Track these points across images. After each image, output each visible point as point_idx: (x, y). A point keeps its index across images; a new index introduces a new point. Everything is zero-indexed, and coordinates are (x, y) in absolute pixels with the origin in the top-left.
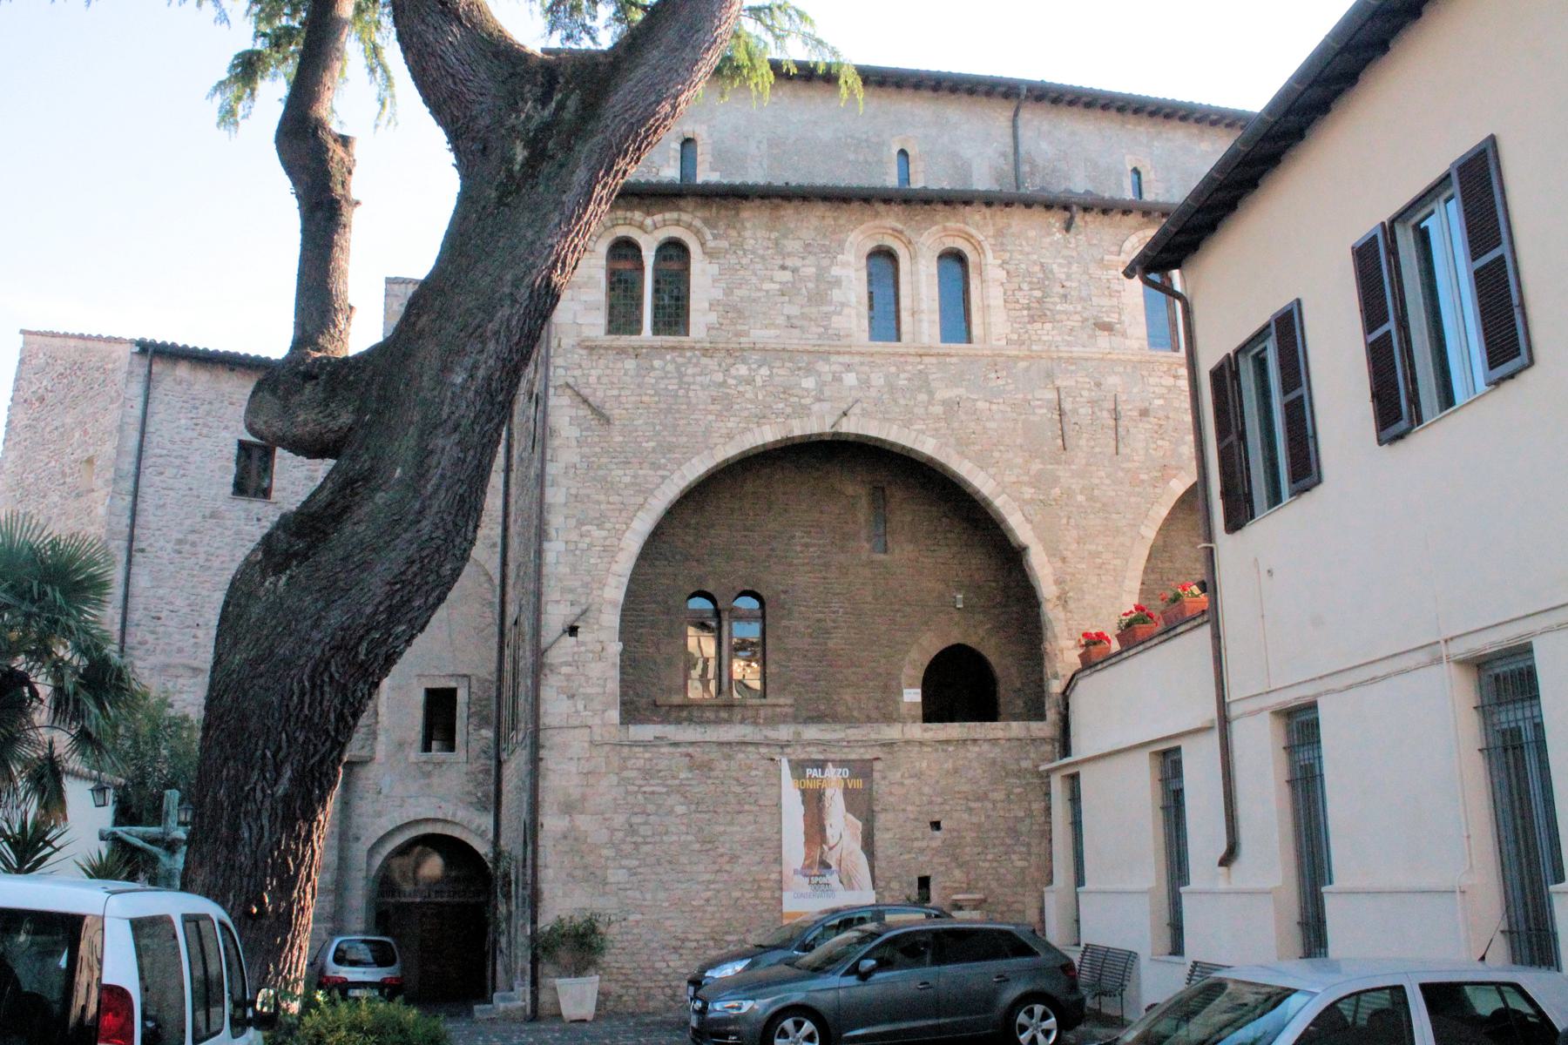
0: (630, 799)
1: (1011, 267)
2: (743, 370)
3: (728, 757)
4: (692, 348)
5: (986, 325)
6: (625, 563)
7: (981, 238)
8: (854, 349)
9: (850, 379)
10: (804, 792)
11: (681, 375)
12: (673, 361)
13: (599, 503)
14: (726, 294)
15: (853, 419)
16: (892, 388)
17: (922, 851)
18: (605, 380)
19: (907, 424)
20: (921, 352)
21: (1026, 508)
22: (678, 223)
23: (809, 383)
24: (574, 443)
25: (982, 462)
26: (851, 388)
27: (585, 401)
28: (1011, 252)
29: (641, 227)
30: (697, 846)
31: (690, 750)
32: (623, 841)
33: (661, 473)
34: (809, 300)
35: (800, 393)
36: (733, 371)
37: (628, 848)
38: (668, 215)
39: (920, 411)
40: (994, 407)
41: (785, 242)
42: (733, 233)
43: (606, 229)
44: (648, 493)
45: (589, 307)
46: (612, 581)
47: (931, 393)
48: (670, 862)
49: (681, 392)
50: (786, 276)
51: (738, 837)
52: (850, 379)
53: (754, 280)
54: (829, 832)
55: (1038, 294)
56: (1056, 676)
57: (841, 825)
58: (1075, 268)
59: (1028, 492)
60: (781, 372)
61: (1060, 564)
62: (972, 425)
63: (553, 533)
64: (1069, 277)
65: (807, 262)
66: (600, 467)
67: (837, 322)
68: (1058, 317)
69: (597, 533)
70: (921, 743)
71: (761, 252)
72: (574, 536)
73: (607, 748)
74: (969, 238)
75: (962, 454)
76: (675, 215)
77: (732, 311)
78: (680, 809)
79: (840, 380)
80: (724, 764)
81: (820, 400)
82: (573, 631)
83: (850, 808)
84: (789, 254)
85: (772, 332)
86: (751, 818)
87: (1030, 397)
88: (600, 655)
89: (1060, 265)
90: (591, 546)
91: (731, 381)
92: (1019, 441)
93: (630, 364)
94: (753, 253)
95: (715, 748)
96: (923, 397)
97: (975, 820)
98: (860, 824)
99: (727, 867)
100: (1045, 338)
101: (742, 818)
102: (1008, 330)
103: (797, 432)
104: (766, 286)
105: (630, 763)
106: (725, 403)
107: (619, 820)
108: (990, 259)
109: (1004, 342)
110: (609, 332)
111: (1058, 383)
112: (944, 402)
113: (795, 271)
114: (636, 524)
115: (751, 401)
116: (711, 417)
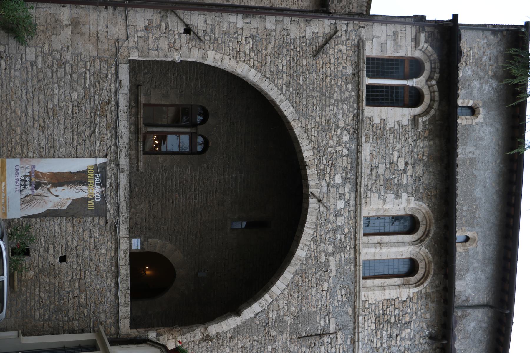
0: (81, 64)
1: (408, 303)
2: (346, 139)
3: (108, 126)
4: (358, 108)
5: (373, 288)
6: (229, 64)
7: (425, 285)
8: (358, 207)
9: (341, 204)
10: (85, 172)
11: (343, 101)
12: (351, 96)
13: (266, 49)
14: (390, 129)
15: (317, 206)
16: (335, 230)
17: (47, 251)
18: (340, 55)
20: (357, 248)
21: (263, 315)
22: (432, 100)
23: (338, 179)
24: (302, 35)
25: (292, 286)
26: (335, 205)
27: (327, 42)
28: (417, 303)
29: (430, 79)
30: (50, 105)
31: (113, 103)
32: (54, 58)
33: (284, 87)
34: (387, 180)
35: (332, 174)
36: (345, 133)
37: (49, 61)
38: (437, 94)
39: (322, 247)
40: (325, 293)
41: (421, 165)
42: (426, 134)
43: (429, 57)
44: (272, 79)
45: (382, 46)
46: (218, 56)
47: (333, 254)
48: (40, 88)
49: (332, 101)
50: (401, 166)
51: (56, 131)
52: (341, 204)
53: (399, 146)
54: (60, 188)
55: (393, 320)
56: (159, 335)
57: (65, 196)
58: (409, 342)
59: (273, 315)
60: (345, 162)
61: (229, 336)
62: (314, 280)
63: (248, 20)
64: (402, 339)
65: (410, 178)
66: (287, 50)
67: (374, 196)
68: (379, 333)
69: (247, 48)
70: (116, 250)
71: (415, 150)
72: (246, 33)
73: (114, 50)
74: (425, 277)
75: (296, 273)
76: (437, 98)
77: (381, 132)
78: (75, 96)
79: (340, 198)
80: (103, 124)
81: (328, 186)
82: (188, 31)
83: (75, 202)
84: (413, 167)
85: (368, 158)
86: (69, 140)
87: (331, 315)
88: (172, 47)
89: (410, 333)
90: (240, 43)
91: (339, 131)
92: (304, 309)
93: (349, 70)
94: (415, 146)
95: (114, 118)
96: (330, 249)
97: (67, 284)
98: (65, 208)
99: (36, 124)
100: (366, 324)
101: (69, 134)
102: (370, 301)
103: (309, 172)
104: (396, 154)
105: (104, 64)
106: (327, 128)
107: (68, 56)
108: (413, 290)
109: (363, 299)
110: (368, 59)
111: (340, 333)
112: (327, 261)
113: (405, 171)
114: (253, 71)
115: (327, 143)
116: (317, 118)
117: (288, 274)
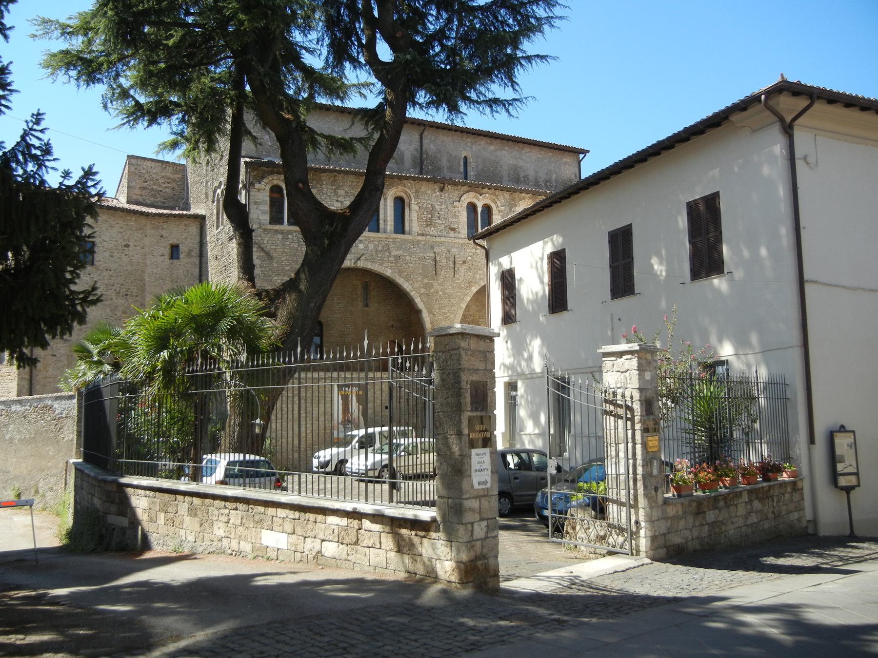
19: (381, 264)
45: (263, 212)
55: (429, 216)
59: (423, 291)
64: (441, 209)
75: (400, 276)
93: (280, 236)
117: (400, 281)
